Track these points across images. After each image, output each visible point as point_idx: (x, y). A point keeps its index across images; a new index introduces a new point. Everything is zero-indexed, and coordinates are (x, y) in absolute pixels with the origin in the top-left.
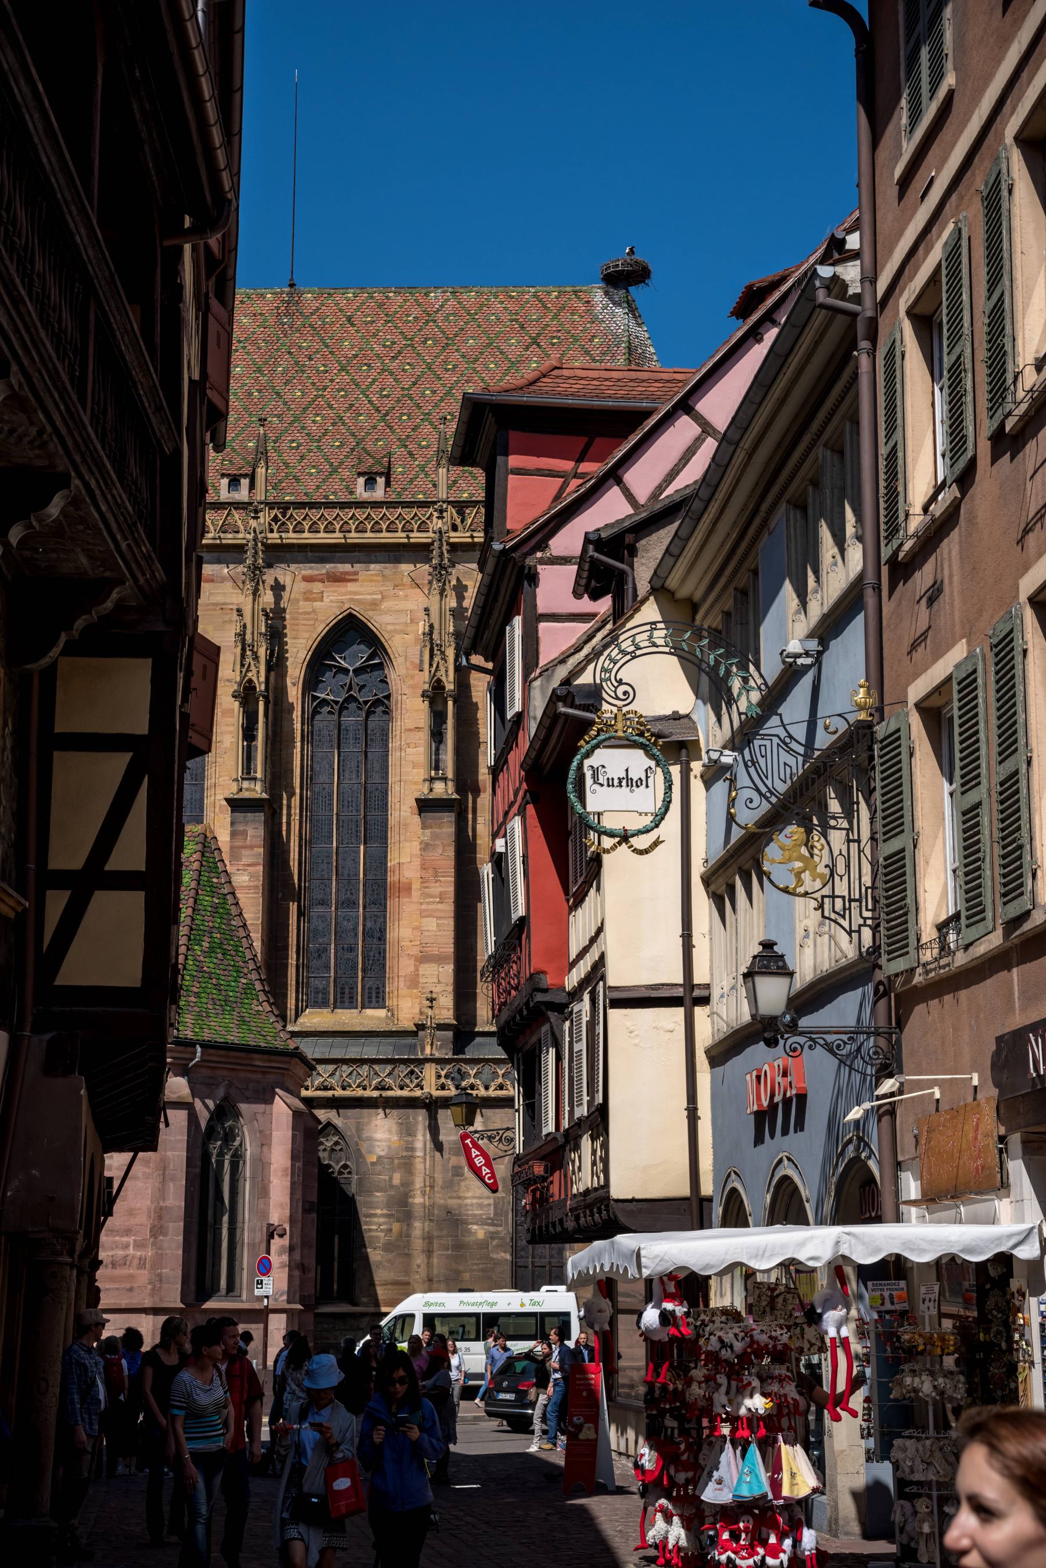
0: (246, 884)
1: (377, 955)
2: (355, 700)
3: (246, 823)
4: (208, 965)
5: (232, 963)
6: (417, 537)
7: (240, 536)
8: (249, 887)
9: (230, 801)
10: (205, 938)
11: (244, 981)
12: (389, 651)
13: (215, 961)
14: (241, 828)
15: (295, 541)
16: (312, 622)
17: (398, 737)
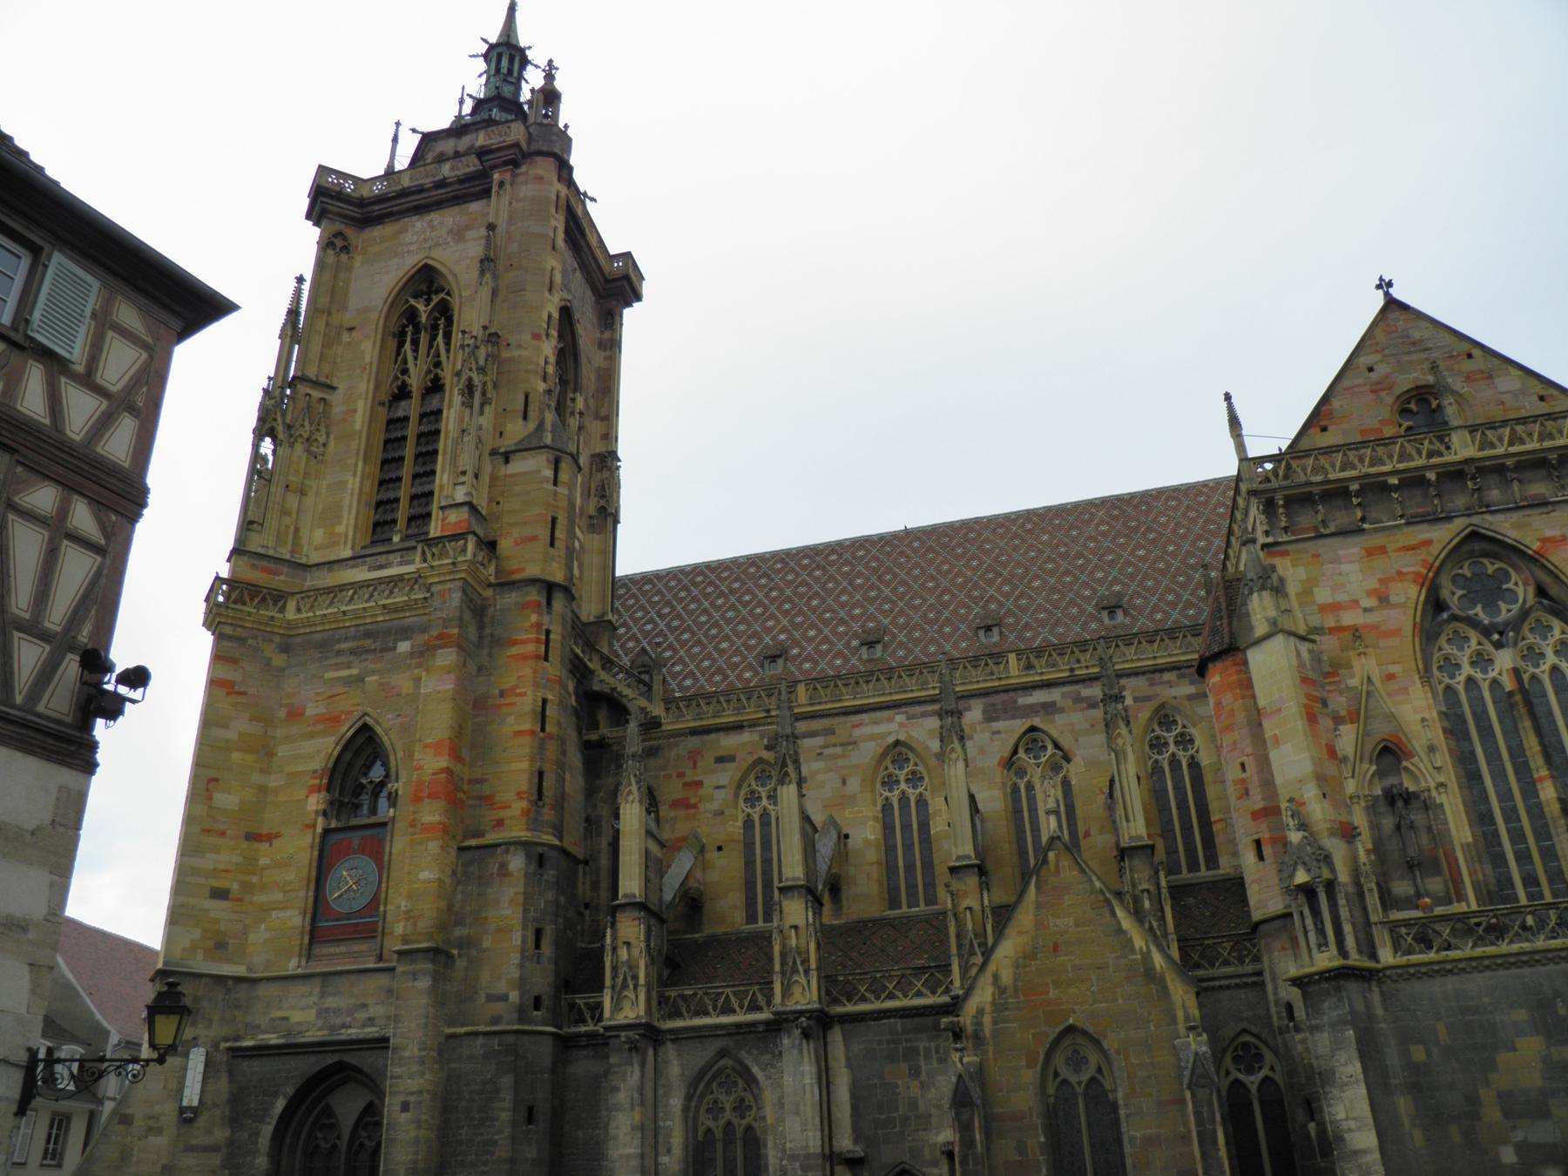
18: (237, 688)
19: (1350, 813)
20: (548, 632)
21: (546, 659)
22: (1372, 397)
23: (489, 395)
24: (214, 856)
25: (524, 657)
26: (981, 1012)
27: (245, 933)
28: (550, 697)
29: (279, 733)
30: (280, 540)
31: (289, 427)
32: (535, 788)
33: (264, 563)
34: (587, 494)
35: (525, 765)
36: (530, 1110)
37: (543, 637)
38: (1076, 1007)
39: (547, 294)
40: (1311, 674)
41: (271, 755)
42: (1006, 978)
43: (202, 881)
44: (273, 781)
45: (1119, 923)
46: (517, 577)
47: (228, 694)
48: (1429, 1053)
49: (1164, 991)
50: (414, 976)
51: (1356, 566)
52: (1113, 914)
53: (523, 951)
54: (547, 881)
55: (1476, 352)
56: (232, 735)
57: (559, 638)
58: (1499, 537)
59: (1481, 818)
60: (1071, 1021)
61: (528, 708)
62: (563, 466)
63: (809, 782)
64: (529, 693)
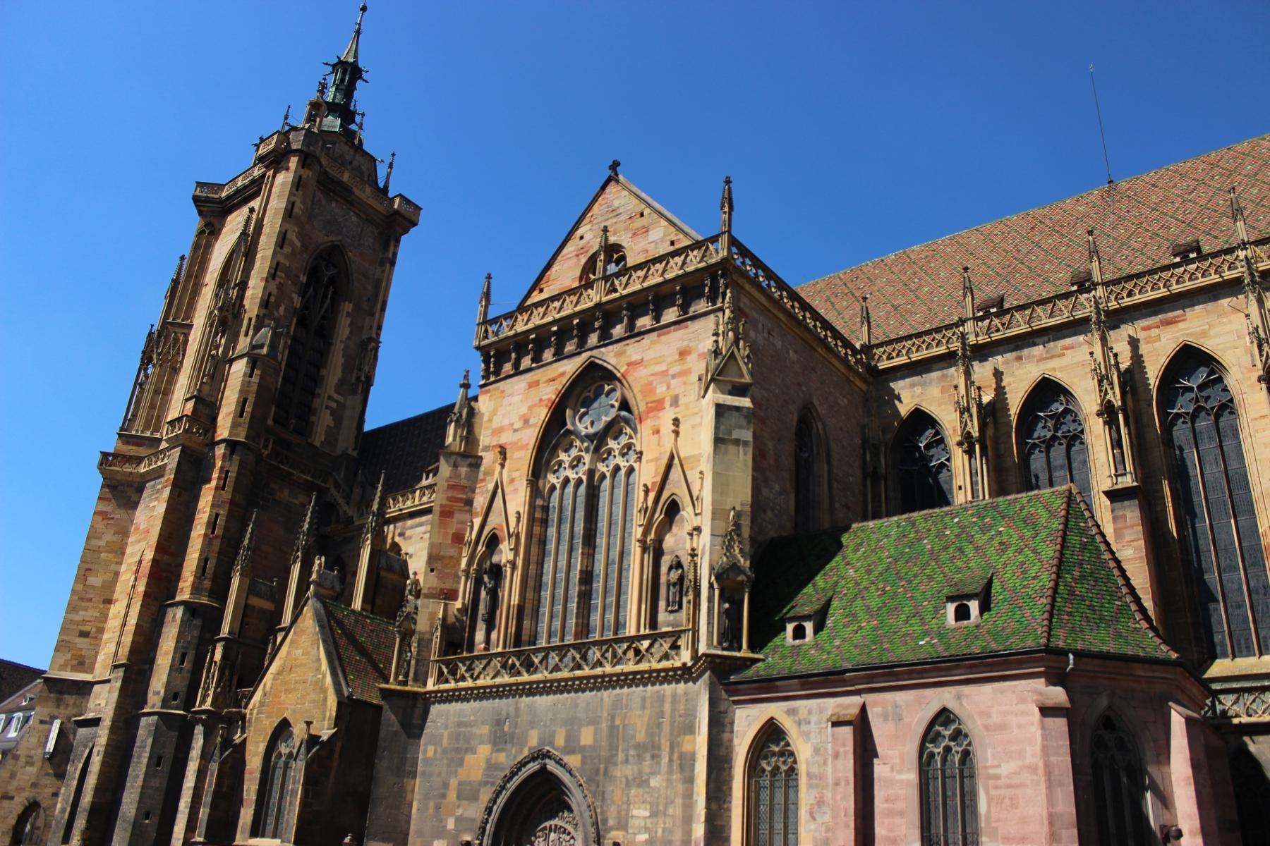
0: (1132, 556)
1: (1265, 609)
2: (1203, 408)
3: (1124, 508)
4: (1080, 589)
5: (1105, 588)
6: (1228, 275)
7: (1087, 310)
8: (1135, 559)
9: (1109, 494)
10: (1076, 568)
11: (1119, 603)
12: (1224, 364)
13: (1087, 586)
14: (1119, 513)
15: (1130, 303)
16: (1155, 358)
17: (1247, 428)
18: (109, 516)
19: (459, 582)
20: (227, 472)
21: (223, 489)
22: (575, 259)
23: (230, 324)
24: (84, 613)
25: (211, 489)
26: (254, 705)
27: (96, 657)
28: (222, 512)
29: (130, 540)
30: (147, 427)
31: (159, 354)
32: (201, 568)
33: (135, 440)
34: (347, 367)
35: (197, 555)
36: (160, 759)
37: (224, 475)
38: (289, 707)
39: (278, 249)
40: (463, 482)
41: (123, 553)
42: (268, 687)
43: (75, 627)
44: (123, 568)
45: (319, 653)
46: (218, 439)
47: (103, 519)
48: (435, 751)
49: (325, 699)
50: (117, 678)
51: (521, 396)
52: (318, 648)
53: (172, 665)
54: (195, 625)
55: (647, 211)
56: (102, 543)
57: (235, 475)
58: (605, 364)
59: (532, 583)
60: (285, 715)
61: (206, 520)
62: (258, 363)
63: (414, 557)
64: (208, 509)
